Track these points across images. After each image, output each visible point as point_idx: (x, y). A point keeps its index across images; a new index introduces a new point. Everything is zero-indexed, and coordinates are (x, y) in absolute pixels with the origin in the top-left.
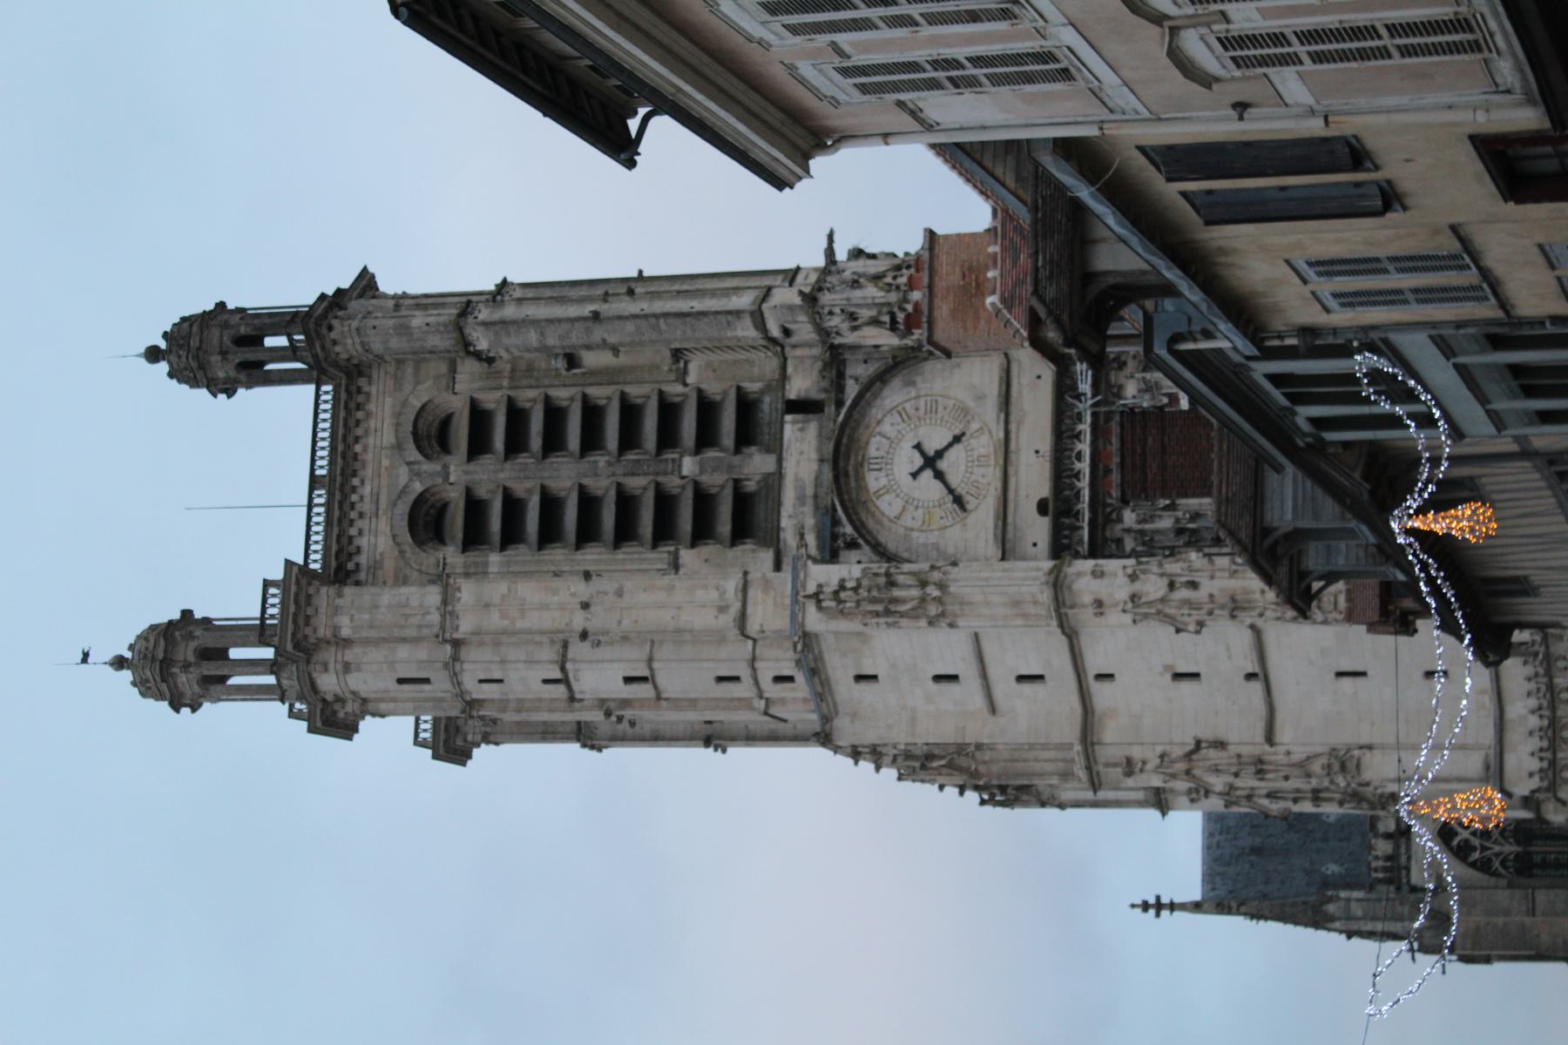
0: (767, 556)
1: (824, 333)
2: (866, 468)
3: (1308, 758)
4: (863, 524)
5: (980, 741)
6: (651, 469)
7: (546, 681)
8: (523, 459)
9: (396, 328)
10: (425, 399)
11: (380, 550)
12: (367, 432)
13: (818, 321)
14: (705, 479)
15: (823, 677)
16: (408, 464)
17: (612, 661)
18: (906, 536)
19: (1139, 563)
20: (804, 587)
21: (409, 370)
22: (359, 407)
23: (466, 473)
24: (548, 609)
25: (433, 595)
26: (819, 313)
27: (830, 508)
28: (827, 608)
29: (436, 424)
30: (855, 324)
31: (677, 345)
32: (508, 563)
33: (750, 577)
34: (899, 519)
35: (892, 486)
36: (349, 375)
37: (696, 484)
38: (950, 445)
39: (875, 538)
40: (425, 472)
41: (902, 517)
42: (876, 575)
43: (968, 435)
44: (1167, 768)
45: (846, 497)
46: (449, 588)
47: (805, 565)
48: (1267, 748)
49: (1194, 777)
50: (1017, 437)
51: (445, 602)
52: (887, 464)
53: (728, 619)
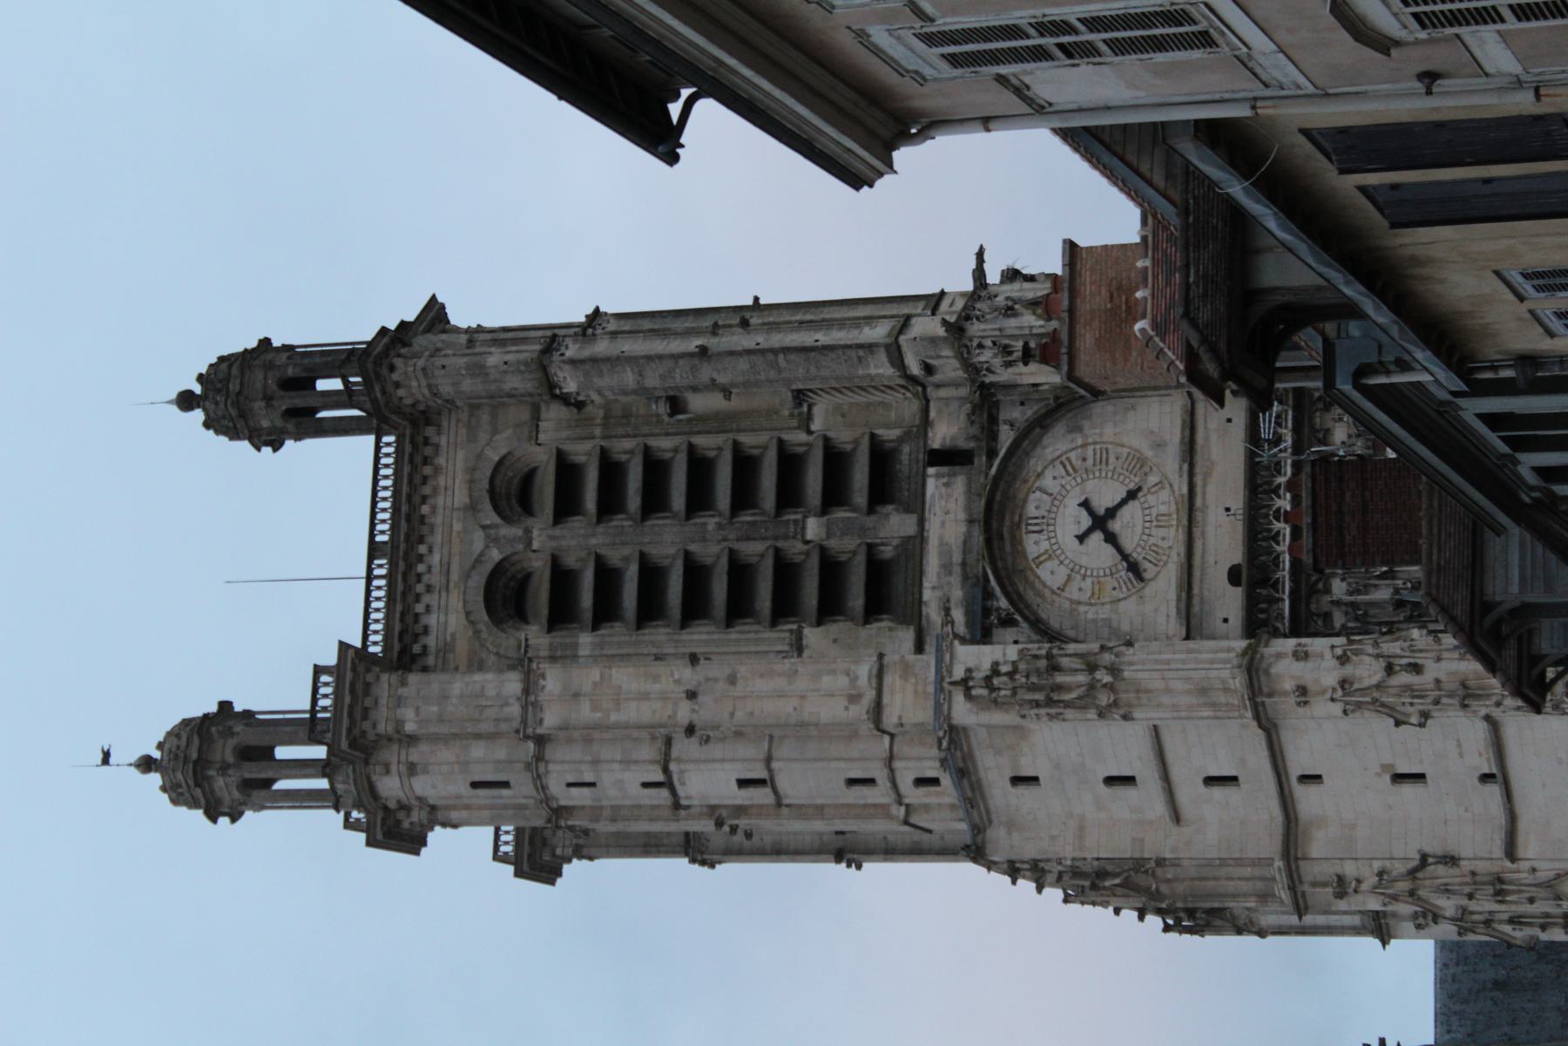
0: (907, 636)
1: (973, 370)
2: (1024, 531)
3: (1559, 876)
4: (1020, 596)
5: (1163, 856)
6: (770, 533)
7: (646, 785)
8: (619, 521)
9: (468, 368)
10: (503, 451)
11: (451, 629)
12: (435, 490)
13: (965, 355)
14: (833, 543)
15: (973, 778)
16: (484, 527)
17: (723, 760)
18: (1072, 611)
19: (1351, 642)
20: (950, 673)
21: (485, 417)
22: (426, 461)
23: (552, 538)
24: (648, 699)
25: (512, 684)
26: (967, 346)
27: (980, 575)
28: (978, 697)
29: (516, 481)
30: (1010, 358)
31: (800, 386)
32: (601, 645)
33: (886, 660)
34: (1063, 590)
35: (1054, 551)
36: (414, 423)
37: (823, 550)
38: (1123, 502)
39: (1035, 614)
40: (504, 537)
41: (1067, 589)
42: (1036, 657)
43: (1145, 490)
44: (1386, 888)
45: (1000, 564)
46: (532, 676)
47: (952, 643)
48: (1508, 864)
49: (1419, 898)
50: (1204, 493)
51: (526, 691)
52: (1048, 525)
53: (860, 711)
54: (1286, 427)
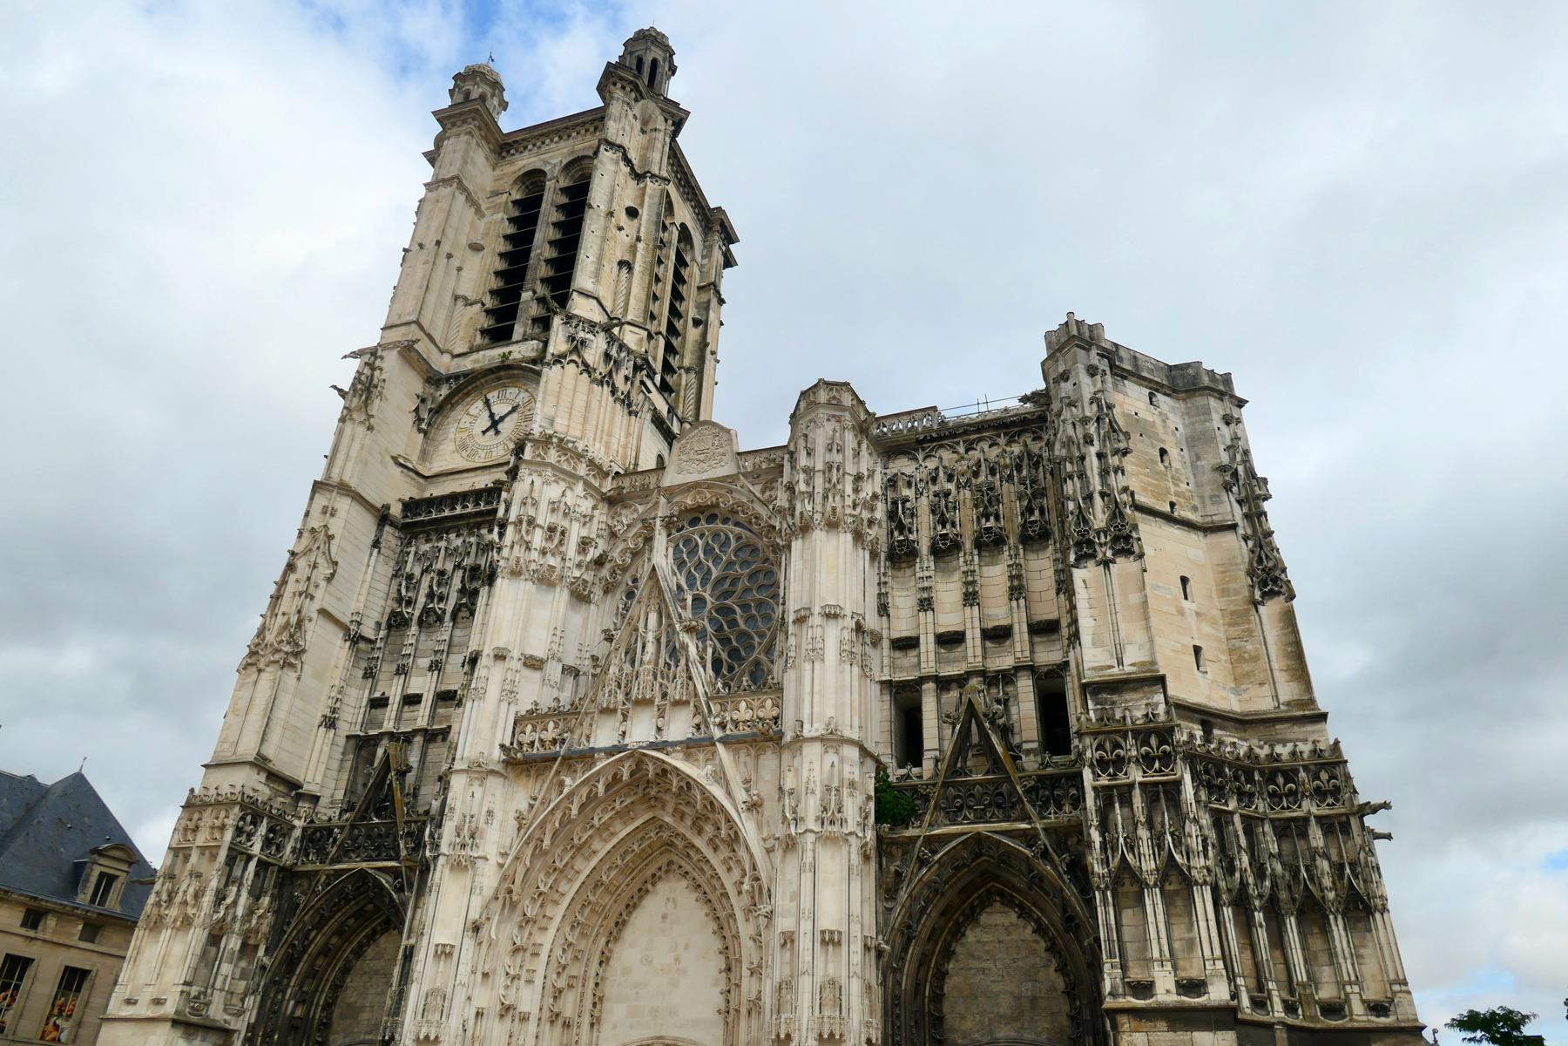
4: (468, 395)
39: (457, 403)
45: (482, 380)
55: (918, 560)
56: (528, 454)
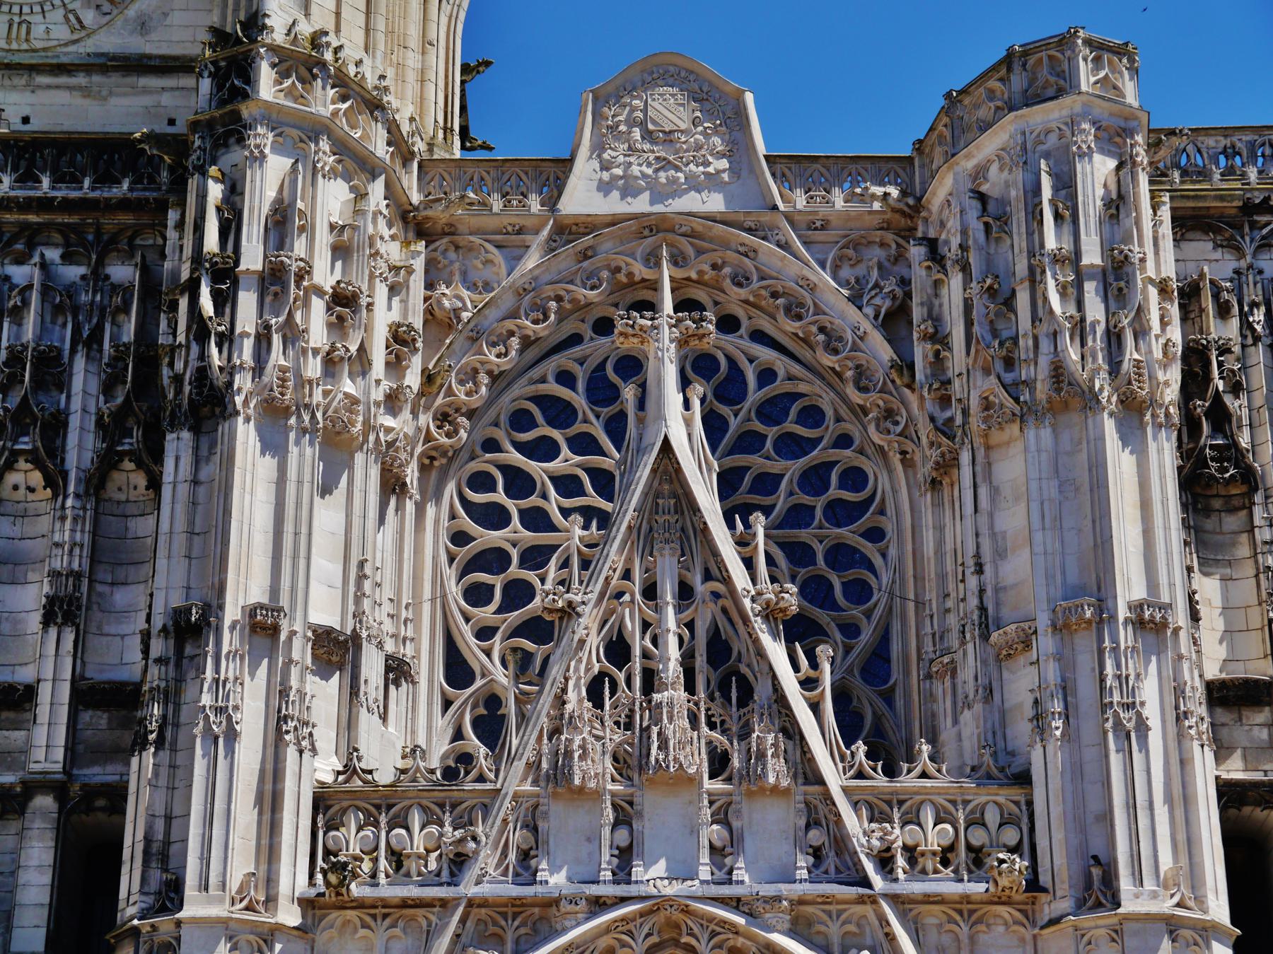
50: (58, 87)
54: (131, 189)
55: (1258, 498)
56: (267, 85)
